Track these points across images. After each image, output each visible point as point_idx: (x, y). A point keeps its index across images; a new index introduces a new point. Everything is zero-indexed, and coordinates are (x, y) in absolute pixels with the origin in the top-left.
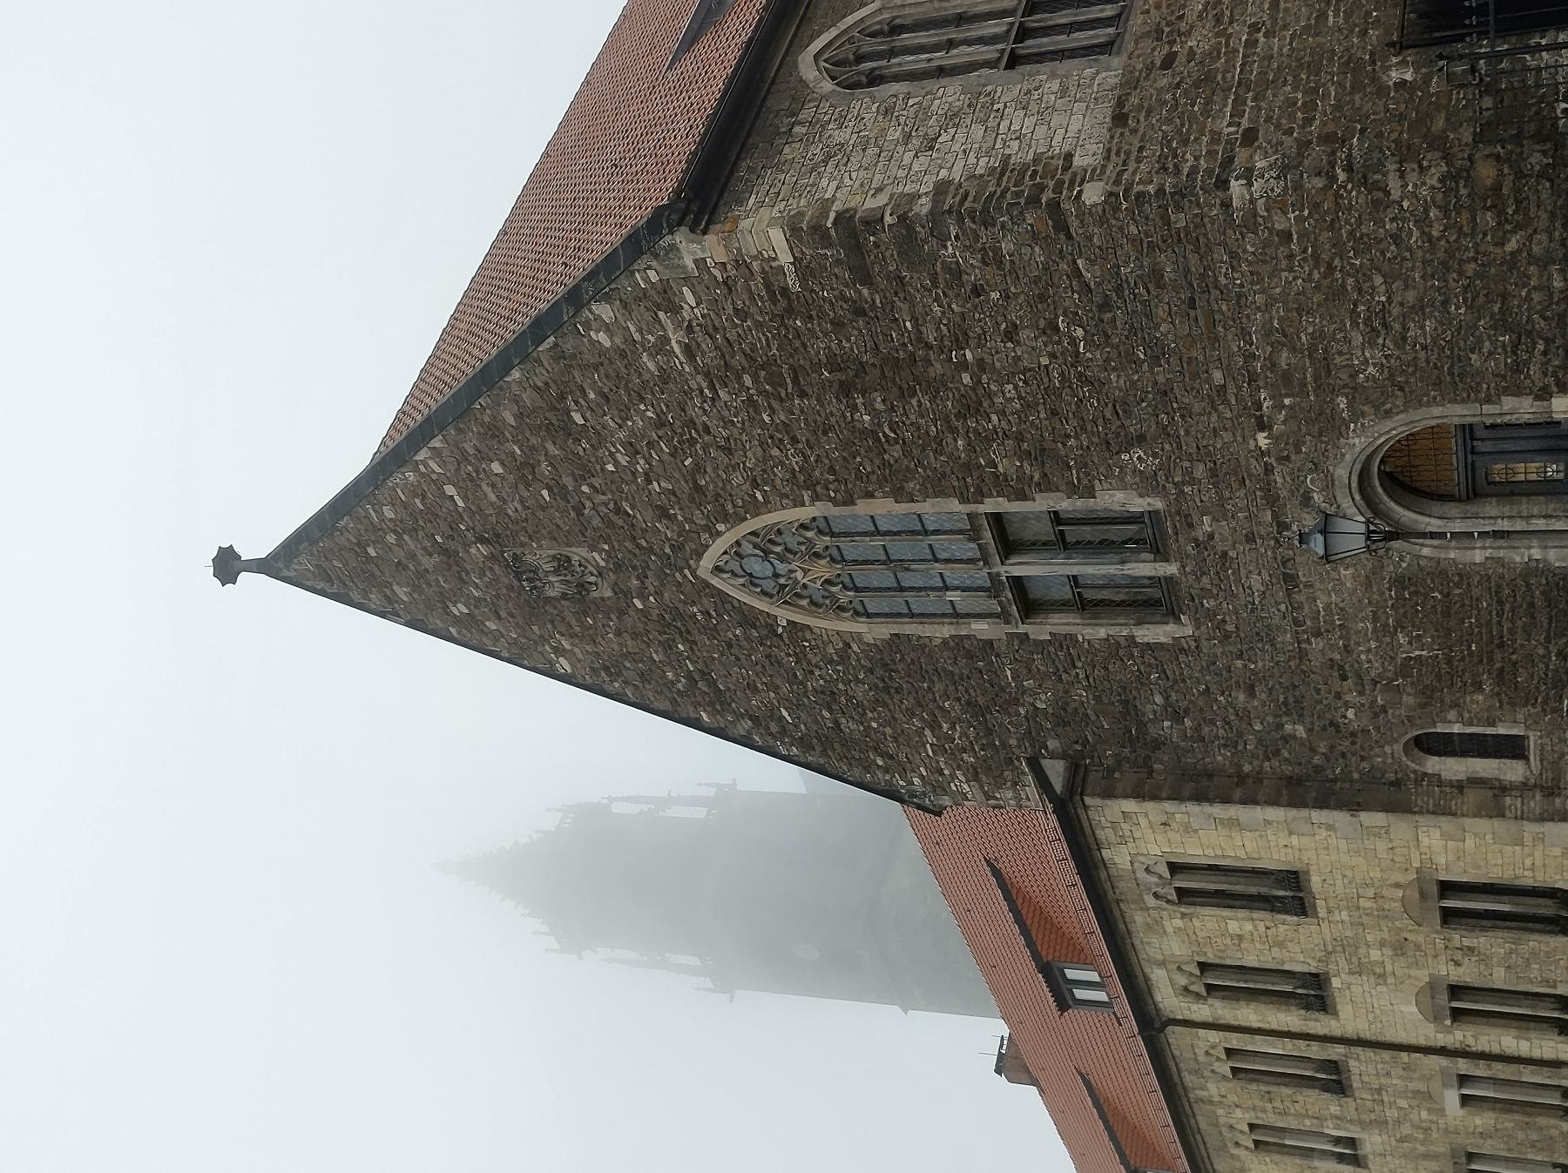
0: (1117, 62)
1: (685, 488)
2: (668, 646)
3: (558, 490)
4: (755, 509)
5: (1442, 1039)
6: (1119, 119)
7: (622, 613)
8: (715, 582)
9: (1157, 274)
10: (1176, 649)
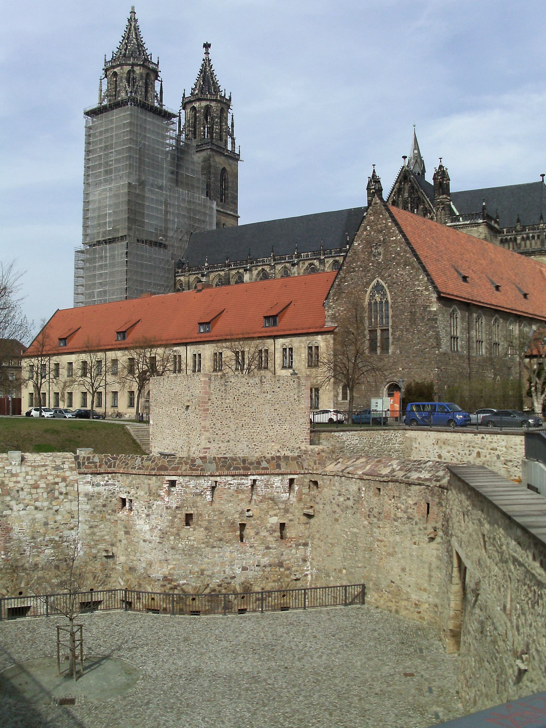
0: (450, 352)
1: (394, 281)
2: (361, 266)
3: (394, 258)
4: (390, 292)
6: (445, 354)
7: (369, 260)
8: (375, 280)
9: (425, 358)
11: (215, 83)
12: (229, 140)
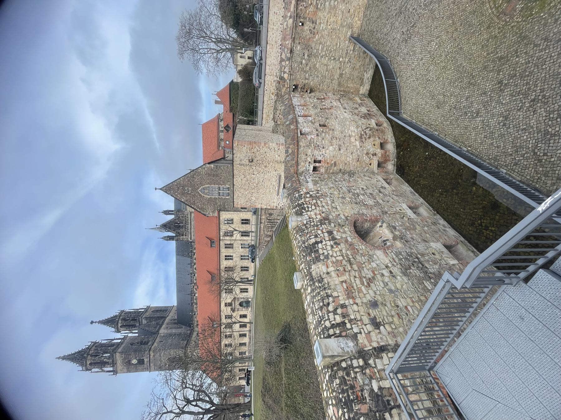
3: (191, 182)
4: (204, 185)
5: (240, 239)
10: (228, 199)
11: (112, 318)
12: (140, 310)
